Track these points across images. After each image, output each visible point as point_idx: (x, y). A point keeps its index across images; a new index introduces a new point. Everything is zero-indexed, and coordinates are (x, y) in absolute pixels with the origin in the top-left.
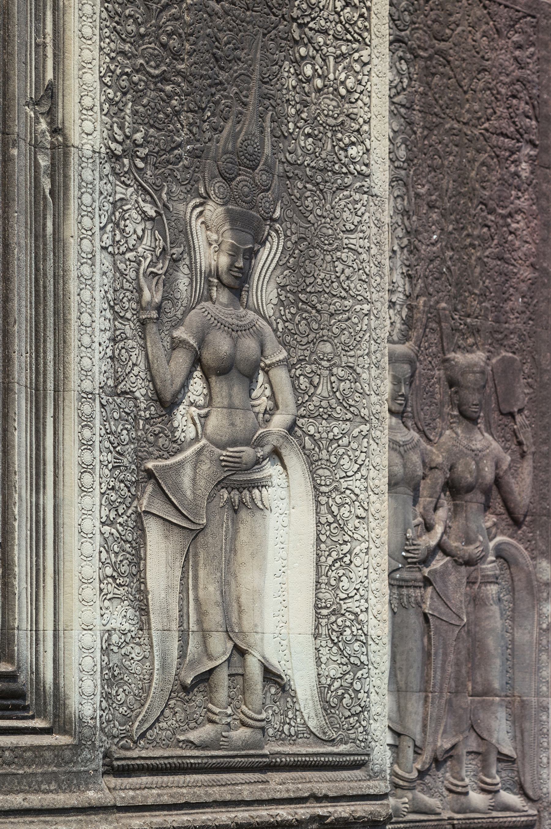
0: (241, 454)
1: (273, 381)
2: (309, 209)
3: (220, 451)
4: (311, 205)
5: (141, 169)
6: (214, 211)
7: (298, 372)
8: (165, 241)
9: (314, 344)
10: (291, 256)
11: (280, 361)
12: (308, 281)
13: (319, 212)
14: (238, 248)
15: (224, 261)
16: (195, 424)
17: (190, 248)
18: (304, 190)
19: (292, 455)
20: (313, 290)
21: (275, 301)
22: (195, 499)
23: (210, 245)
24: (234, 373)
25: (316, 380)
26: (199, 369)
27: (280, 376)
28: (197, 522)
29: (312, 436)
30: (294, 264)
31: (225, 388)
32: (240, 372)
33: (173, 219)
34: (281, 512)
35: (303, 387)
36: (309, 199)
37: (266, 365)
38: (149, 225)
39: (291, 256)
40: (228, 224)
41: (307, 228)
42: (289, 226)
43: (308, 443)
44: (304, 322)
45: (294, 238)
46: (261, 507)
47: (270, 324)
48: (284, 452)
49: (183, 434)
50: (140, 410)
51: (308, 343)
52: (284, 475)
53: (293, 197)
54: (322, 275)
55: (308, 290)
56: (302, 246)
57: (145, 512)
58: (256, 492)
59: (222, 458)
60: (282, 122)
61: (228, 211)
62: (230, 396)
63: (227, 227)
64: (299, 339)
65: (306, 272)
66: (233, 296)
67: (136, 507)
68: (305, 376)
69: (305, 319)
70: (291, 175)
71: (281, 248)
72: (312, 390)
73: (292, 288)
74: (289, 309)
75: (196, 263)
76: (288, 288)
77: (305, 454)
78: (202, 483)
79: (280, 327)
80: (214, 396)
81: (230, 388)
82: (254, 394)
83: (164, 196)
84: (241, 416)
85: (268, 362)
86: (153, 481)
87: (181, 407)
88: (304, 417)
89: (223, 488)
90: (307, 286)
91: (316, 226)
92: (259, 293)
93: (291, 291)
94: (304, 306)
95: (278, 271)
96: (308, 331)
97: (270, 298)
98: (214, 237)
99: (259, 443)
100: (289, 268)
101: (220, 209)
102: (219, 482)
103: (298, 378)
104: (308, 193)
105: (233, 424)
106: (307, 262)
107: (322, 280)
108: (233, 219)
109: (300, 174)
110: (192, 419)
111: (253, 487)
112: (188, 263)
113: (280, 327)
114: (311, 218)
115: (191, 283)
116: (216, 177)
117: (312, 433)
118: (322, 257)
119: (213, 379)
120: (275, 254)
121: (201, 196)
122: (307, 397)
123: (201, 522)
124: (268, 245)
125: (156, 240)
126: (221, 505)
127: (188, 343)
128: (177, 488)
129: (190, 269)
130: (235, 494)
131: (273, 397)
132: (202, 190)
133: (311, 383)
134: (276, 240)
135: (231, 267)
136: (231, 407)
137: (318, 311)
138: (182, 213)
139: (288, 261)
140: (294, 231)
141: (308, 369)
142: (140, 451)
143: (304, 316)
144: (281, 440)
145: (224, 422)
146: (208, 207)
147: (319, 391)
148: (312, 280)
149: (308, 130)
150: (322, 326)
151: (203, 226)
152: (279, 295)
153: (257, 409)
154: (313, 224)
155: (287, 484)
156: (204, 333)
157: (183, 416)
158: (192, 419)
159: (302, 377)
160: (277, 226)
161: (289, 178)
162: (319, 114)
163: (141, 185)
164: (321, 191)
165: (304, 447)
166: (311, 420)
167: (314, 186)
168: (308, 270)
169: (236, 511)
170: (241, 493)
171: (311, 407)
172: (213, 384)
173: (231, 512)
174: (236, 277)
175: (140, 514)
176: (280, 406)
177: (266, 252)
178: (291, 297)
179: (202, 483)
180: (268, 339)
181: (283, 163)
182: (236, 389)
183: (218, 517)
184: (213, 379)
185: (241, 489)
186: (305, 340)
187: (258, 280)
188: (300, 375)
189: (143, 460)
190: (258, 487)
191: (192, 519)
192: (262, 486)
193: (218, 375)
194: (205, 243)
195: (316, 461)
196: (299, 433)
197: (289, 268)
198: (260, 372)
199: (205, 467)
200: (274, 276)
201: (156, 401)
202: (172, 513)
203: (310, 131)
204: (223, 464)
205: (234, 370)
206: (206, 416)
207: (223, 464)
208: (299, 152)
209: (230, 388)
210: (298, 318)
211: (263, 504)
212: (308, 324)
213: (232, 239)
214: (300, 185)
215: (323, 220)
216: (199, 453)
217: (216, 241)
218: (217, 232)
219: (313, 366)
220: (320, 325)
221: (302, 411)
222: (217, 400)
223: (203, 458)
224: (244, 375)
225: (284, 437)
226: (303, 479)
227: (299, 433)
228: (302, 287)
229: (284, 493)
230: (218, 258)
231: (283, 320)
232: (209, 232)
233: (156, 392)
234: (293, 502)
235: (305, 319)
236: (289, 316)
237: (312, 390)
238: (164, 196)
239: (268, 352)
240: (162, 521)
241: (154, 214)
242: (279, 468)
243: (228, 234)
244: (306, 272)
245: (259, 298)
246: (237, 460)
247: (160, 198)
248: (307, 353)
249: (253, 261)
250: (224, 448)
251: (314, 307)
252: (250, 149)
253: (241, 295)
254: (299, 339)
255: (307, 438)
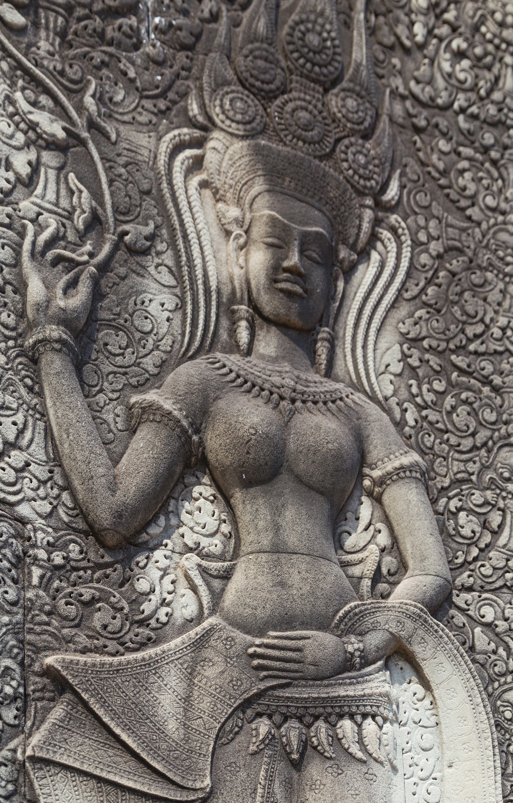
0: (301, 643)
1: (391, 514)
2: (468, 193)
3: (249, 638)
4: (472, 188)
5: (21, 31)
6: (226, 153)
7: (454, 504)
8: (97, 195)
9: (489, 451)
10: (429, 282)
11: (402, 468)
12: (470, 331)
13: (490, 201)
14: (286, 229)
15: (259, 259)
16: (194, 589)
17: (172, 231)
18: (453, 156)
19: (441, 657)
20: (482, 349)
21: (397, 368)
22: (187, 739)
23: (228, 233)
24: (284, 482)
25: (495, 519)
26: (206, 480)
27: (407, 501)
28: (190, 784)
29: (489, 626)
30: (437, 296)
31: (265, 513)
32: (299, 479)
33: (122, 160)
34: (423, 774)
35: (466, 532)
36: (468, 175)
37: (374, 481)
38: (49, 158)
39: (429, 282)
40: (260, 181)
41: (463, 230)
42: (422, 222)
43: (481, 639)
44: (463, 410)
45: (435, 247)
46: (360, 755)
47: (388, 412)
48: (418, 650)
49: (164, 610)
50: (34, 546)
51: (474, 448)
52: (427, 702)
53: (430, 169)
54: (503, 321)
55: (472, 347)
56: (456, 264)
57: (33, 759)
58: (347, 726)
59: (251, 650)
60: (397, 21)
61: (258, 151)
62: (277, 528)
63: (259, 186)
64: (453, 440)
65: (465, 313)
66: (289, 344)
67: (14, 751)
68: (471, 511)
69: (466, 402)
70: (423, 123)
71: (405, 264)
72: (487, 538)
73: (434, 344)
74: (430, 383)
75: (191, 267)
76: (425, 343)
77: (474, 661)
78: (205, 704)
79: (410, 417)
80: (243, 535)
81: (277, 511)
82: (349, 542)
83: (89, 101)
84: (303, 567)
85: (376, 473)
86: (68, 696)
87: (158, 554)
88: (470, 589)
89: (259, 715)
90: (470, 340)
91: (484, 226)
92: (359, 351)
93: (431, 349)
94: (464, 379)
95: (403, 310)
96: (473, 425)
97: (386, 360)
98: (233, 212)
99: (352, 625)
100: (426, 305)
101: (238, 146)
102: (247, 703)
103: (455, 515)
104: (464, 164)
105: (282, 584)
106: (467, 295)
107: (503, 330)
108: (276, 173)
109: (443, 124)
110: (187, 577)
111: (341, 716)
112: (170, 262)
113: (410, 417)
114: (474, 212)
115: (181, 307)
116: (228, 83)
117: (489, 618)
118: (501, 285)
119: (238, 496)
120: (393, 276)
121: (193, 124)
122: (475, 552)
123: (198, 785)
124: (375, 256)
125: (72, 193)
126: (253, 748)
127: (160, 408)
128: (140, 715)
129: (176, 273)
130: (288, 729)
131: (395, 547)
132: (194, 109)
133: (485, 525)
134: (392, 247)
135: (275, 270)
136: (278, 549)
137: (496, 389)
138: (146, 153)
139: (423, 290)
140: (434, 233)
141: (477, 498)
142: (31, 631)
143: (463, 396)
144: (409, 624)
145: (261, 579)
146: (211, 144)
147: (502, 540)
148: (479, 329)
149: (458, 43)
150: (505, 417)
151: (207, 193)
152: (405, 357)
153: (356, 571)
154: (479, 224)
155: (434, 719)
156: (206, 397)
157: (165, 572)
158: (187, 577)
159: (462, 515)
160: (394, 218)
161: (418, 130)
162: (483, 20)
163: (20, 66)
164: (494, 163)
165: (472, 649)
166: (485, 595)
167: (476, 150)
168: (470, 309)
169: (297, 765)
170: (309, 726)
171: (487, 571)
172: (239, 509)
173: (281, 766)
174: (289, 294)
175: (23, 765)
176: (411, 563)
177: (372, 270)
178: (434, 361)
179: (205, 704)
180: (375, 426)
181: (403, 98)
182: (290, 514)
183: (243, 774)
184: (238, 496)
185: (308, 719)
186: (467, 443)
187: (356, 325)
188: (459, 509)
189: (38, 650)
190: (352, 716)
191: (177, 779)
192: (365, 716)
193: (247, 484)
194: (215, 230)
195: (503, 675)
196: (460, 619)
197: (426, 305)
198: (364, 499)
199: (212, 672)
200: (392, 321)
201: (86, 534)
202: (123, 766)
203: (464, 45)
204: (255, 662)
205: (284, 477)
206: (226, 576)
207: (255, 662)
208: (440, 83)
209: (277, 511)
210: (449, 401)
211: (363, 747)
212: (474, 413)
213: (272, 210)
214: (443, 145)
215: (500, 218)
216: (200, 643)
217: (239, 222)
218: (239, 202)
219: (489, 493)
220: (500, 415)
221: (464, 578)
222: (248, 539)
223: (209, 653)
224: (311, 488)
225: (414, 618)
226: (469, 707)
227: (460, 619)
228: (457, 341)
229: (429, 738)
230: (246, 261)
231: (417, 405)
232: (220, 205)
233: (79, 510)
234: (448, 755)
235: (466, 402)
236: (429, 397)
237: (487, 538)
238: (89, 101)
239: (375, 453)
240: (92, 783)
241: (61, 134)
242: (417, 687)
243: (262, 202)
244: (465, 313)
245: (360, 360)
246: (289, 654)
247: (80, 108)
248: (472, 467)
249: (341, 284)
250: (261, 633)
251: (486, 381)
252: (313, 39)
253: (315, 352)
254: (453, 440)
255: (478, 630)
